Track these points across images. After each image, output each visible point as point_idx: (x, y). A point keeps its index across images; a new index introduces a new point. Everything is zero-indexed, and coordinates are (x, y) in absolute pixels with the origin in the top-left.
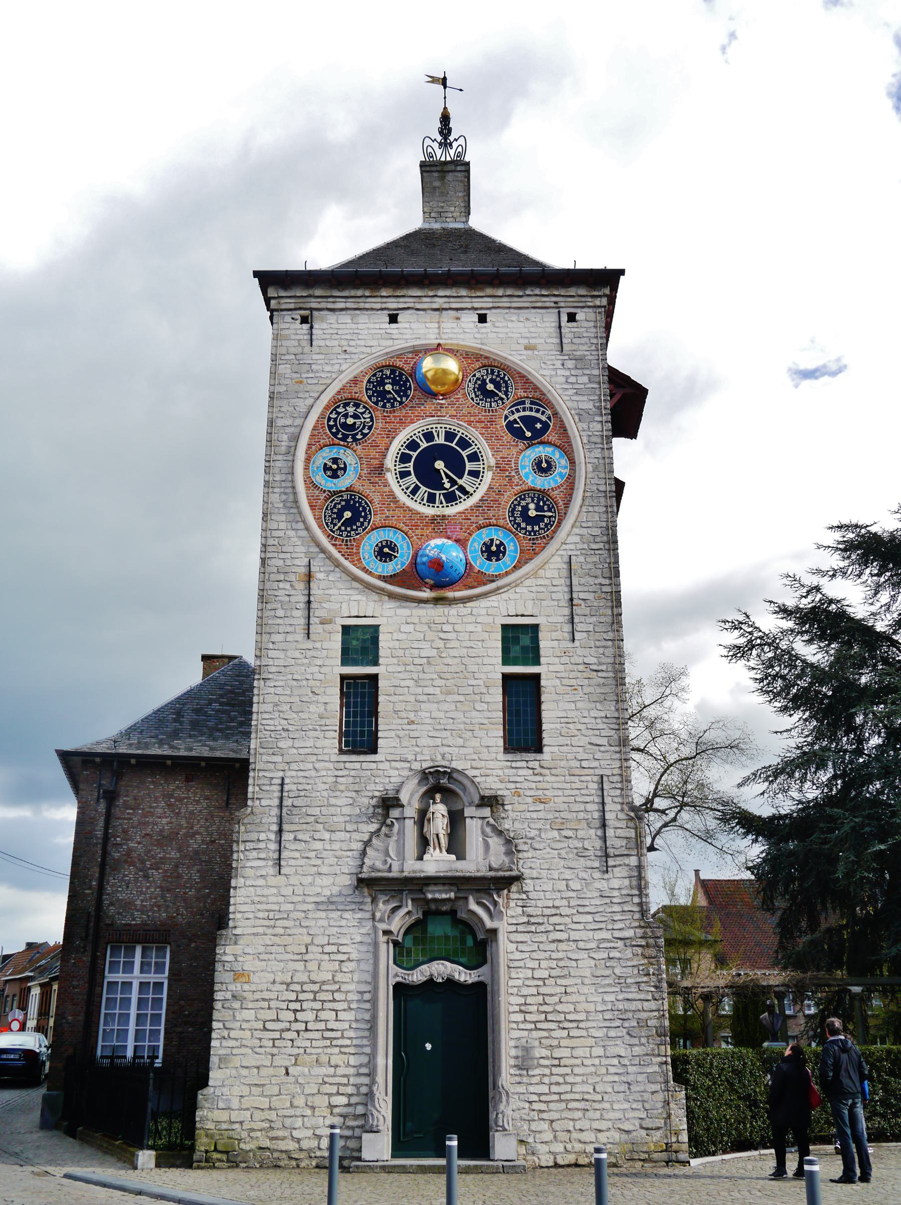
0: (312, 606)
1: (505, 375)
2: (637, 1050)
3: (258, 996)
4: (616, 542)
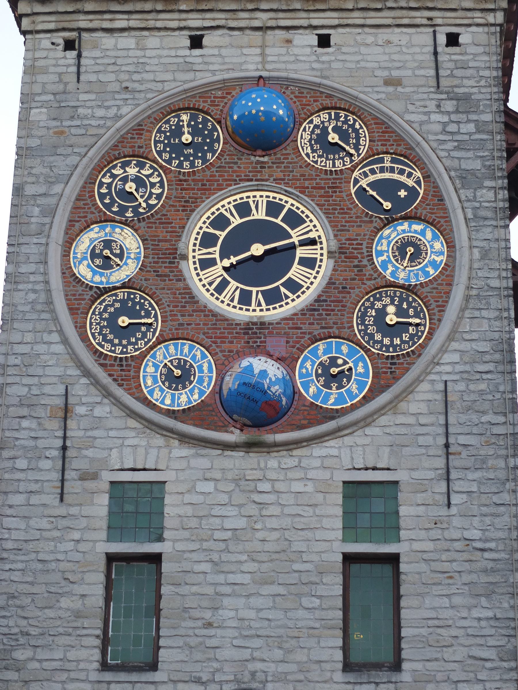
0: (69, 453)
1: (355, 121)
4: (512, 362)
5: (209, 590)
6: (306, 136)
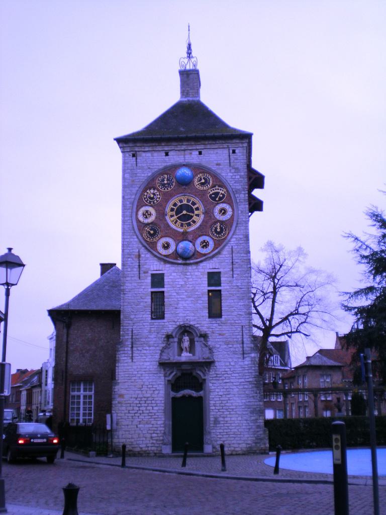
0: (141, 267)
2: (253, 418)
3: (127, 402)
5: (176, 300)
6: (196, 180)
